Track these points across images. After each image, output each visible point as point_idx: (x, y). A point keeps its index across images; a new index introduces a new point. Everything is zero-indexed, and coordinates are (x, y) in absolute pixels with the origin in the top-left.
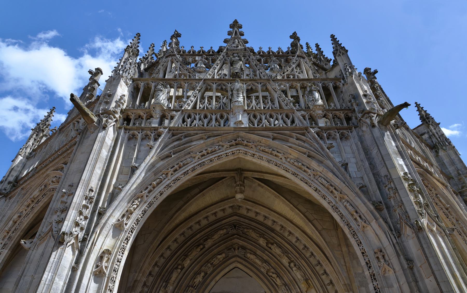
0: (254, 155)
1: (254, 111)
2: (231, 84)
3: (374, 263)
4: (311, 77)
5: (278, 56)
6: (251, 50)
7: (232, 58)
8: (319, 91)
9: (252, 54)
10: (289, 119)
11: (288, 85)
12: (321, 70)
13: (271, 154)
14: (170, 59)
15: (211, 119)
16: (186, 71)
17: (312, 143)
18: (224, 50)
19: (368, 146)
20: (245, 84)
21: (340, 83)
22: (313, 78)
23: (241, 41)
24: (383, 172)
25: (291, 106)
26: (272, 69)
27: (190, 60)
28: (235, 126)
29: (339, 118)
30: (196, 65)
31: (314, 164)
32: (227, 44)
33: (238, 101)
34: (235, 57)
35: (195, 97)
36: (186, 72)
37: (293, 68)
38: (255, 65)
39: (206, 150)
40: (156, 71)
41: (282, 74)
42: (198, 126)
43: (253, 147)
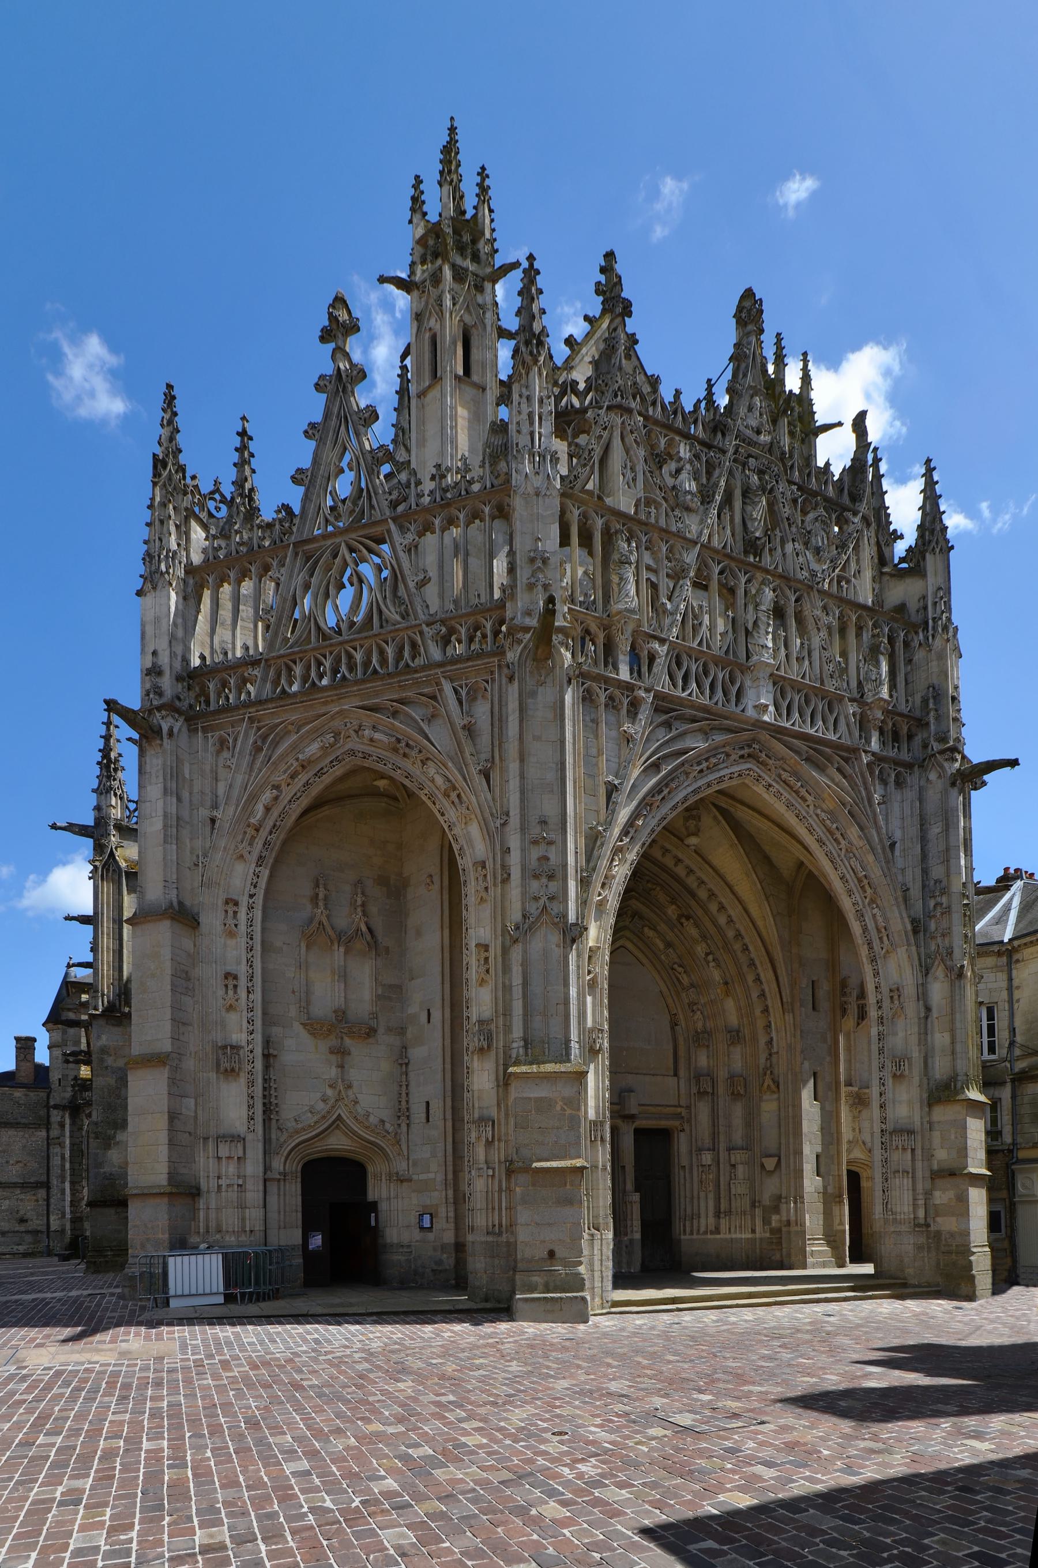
3: (886, 1003)
13: (797, 792)
17: (857, 785)
24: (937, 872)
31: (853, 832)
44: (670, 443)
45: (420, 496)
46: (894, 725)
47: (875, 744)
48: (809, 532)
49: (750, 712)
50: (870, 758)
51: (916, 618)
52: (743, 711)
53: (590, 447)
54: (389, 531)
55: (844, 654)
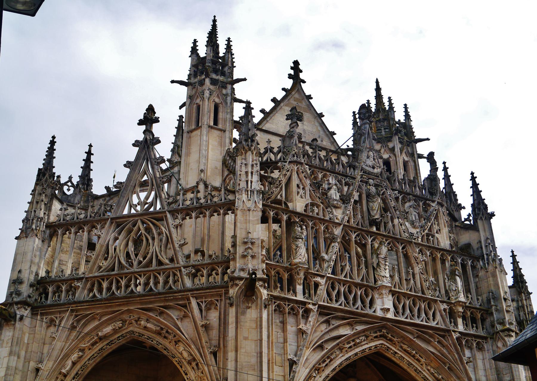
0: (396, 353)
13: (414, 356)
16: (318, 200)
17: (452, 351)
33: (385, 277)
38: (394, 207)
44: (324, 176)
45: (184, 200)
46: (472, 313)
47: (461, 328)
48: (407, 213)
49: (379, 313)
50: (458, 335)
51: (477, 253)
52: (374, 312)
53: (280, 179)
54: (166, 216)
55: (435, 274)
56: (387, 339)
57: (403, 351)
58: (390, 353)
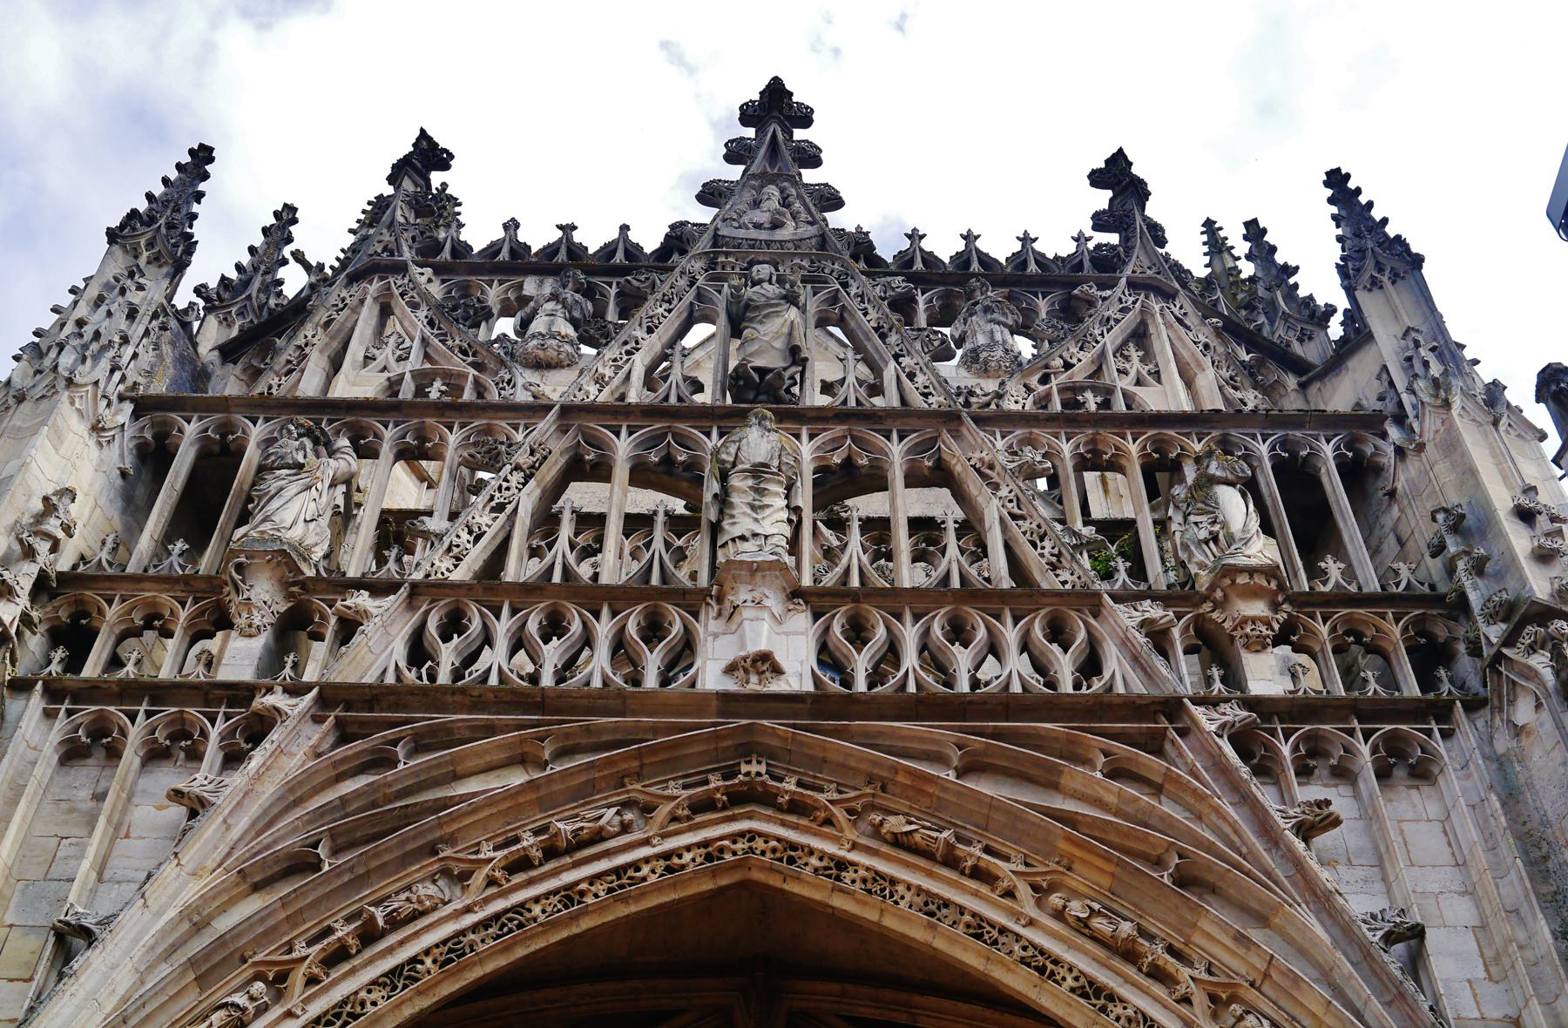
0: (842, 865)
1: (854, 596)
2: (721, 435)
4: (1212, 401)
5: (1017, 283)
6: (857, 244)
7: (737, 288)
8: (1250, 488)
9: (862, 265)
10: (1066, 651)
11: (1066, 448)
12: (1272, 365)
13: (951, 861)
14: (374, 287)
15: (587, 641)
17: (1202, 798)
18: (695, 241)
19: (1546, 823)
20: (812, 437)
21: (1380, 442)
22: (1220, 405)
23: (799, 197)
25: (1078, 571)
26: (973, 360)
27: (493, 294)
28: (730, 685)
29: (1373, 649)
30: (524, 325)
32: (716, 210)
34: (759, 282)
35: (500, 508)
36: (457, 363)
37: (1103, 353)
39: (536, 833)
40: (283, 358)
41: (1034, 381)
42: (501, 681)
43: (839, 814)
56: (779, 808)
57: (885, 849)
58: (808, 870)
